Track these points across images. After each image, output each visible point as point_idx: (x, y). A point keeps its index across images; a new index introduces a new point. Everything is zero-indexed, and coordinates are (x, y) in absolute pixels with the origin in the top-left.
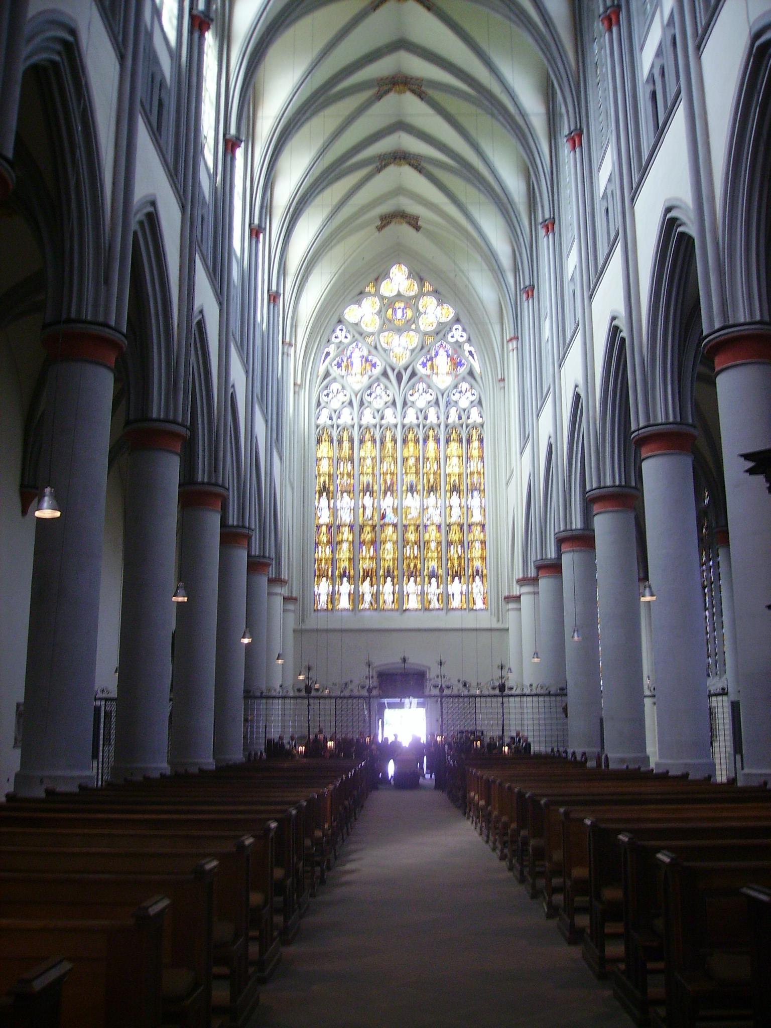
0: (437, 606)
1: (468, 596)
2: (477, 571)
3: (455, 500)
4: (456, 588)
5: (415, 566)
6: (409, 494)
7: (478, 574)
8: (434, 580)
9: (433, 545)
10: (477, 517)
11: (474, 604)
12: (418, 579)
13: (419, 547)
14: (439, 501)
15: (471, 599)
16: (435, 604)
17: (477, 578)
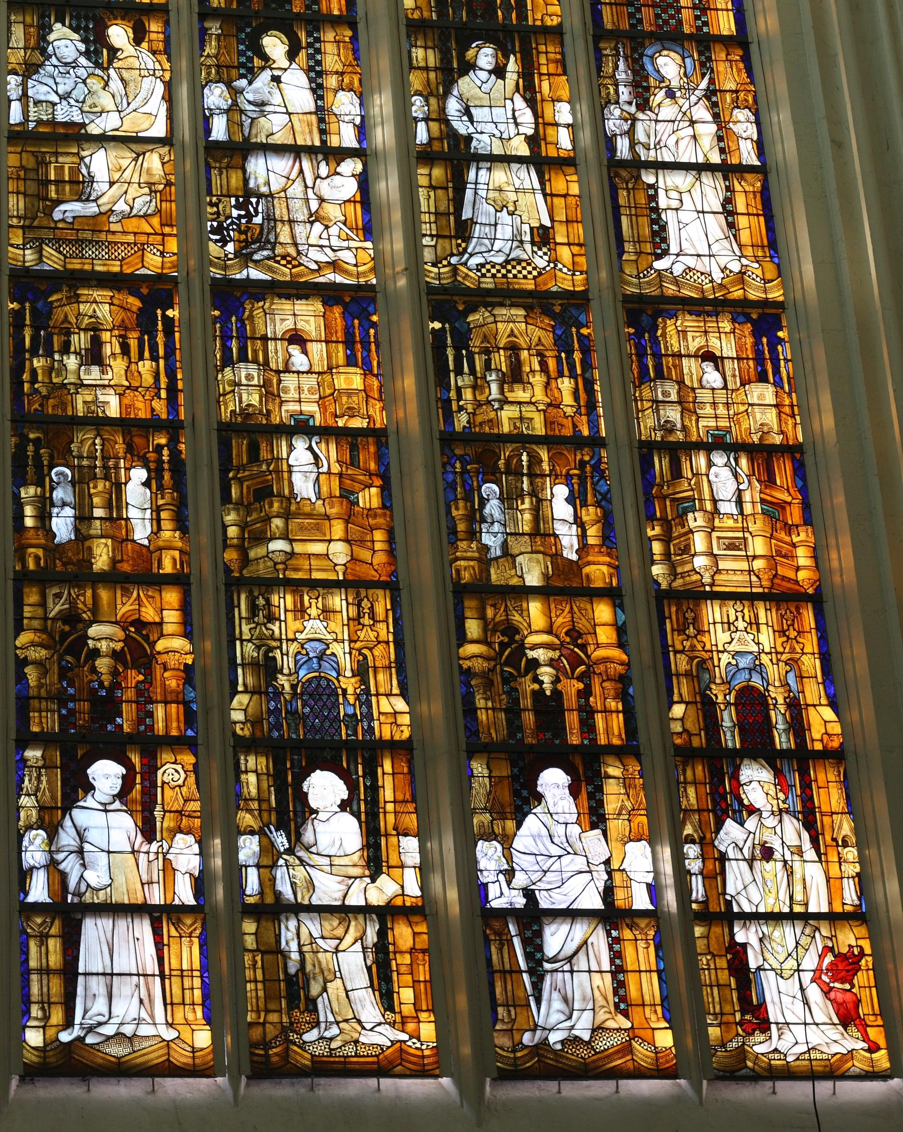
0: (382, 1036)
1: (696, 946)
2: (752, 702)
3: (491, 106)
4: (561, 853)
5: (138, 648)
6: (65, 41)
7: (758, 746)
8: (324, 788)
9: (304, 468)
10: (700, 238)
11: (758, 1019)
12: (173, 772)
13: (170, 479)
14: (345, 104)
15: (714, 970)
16: (355, 1011)
17: (756, 783)
